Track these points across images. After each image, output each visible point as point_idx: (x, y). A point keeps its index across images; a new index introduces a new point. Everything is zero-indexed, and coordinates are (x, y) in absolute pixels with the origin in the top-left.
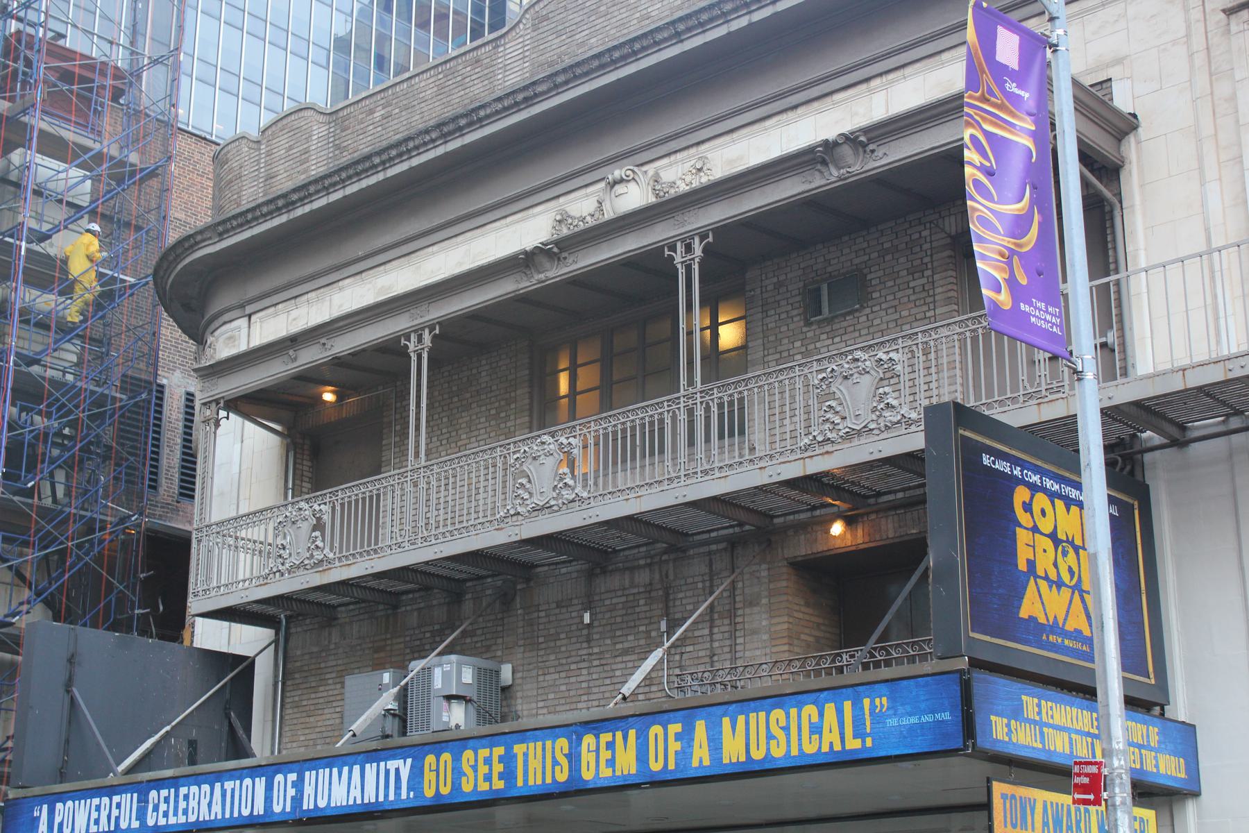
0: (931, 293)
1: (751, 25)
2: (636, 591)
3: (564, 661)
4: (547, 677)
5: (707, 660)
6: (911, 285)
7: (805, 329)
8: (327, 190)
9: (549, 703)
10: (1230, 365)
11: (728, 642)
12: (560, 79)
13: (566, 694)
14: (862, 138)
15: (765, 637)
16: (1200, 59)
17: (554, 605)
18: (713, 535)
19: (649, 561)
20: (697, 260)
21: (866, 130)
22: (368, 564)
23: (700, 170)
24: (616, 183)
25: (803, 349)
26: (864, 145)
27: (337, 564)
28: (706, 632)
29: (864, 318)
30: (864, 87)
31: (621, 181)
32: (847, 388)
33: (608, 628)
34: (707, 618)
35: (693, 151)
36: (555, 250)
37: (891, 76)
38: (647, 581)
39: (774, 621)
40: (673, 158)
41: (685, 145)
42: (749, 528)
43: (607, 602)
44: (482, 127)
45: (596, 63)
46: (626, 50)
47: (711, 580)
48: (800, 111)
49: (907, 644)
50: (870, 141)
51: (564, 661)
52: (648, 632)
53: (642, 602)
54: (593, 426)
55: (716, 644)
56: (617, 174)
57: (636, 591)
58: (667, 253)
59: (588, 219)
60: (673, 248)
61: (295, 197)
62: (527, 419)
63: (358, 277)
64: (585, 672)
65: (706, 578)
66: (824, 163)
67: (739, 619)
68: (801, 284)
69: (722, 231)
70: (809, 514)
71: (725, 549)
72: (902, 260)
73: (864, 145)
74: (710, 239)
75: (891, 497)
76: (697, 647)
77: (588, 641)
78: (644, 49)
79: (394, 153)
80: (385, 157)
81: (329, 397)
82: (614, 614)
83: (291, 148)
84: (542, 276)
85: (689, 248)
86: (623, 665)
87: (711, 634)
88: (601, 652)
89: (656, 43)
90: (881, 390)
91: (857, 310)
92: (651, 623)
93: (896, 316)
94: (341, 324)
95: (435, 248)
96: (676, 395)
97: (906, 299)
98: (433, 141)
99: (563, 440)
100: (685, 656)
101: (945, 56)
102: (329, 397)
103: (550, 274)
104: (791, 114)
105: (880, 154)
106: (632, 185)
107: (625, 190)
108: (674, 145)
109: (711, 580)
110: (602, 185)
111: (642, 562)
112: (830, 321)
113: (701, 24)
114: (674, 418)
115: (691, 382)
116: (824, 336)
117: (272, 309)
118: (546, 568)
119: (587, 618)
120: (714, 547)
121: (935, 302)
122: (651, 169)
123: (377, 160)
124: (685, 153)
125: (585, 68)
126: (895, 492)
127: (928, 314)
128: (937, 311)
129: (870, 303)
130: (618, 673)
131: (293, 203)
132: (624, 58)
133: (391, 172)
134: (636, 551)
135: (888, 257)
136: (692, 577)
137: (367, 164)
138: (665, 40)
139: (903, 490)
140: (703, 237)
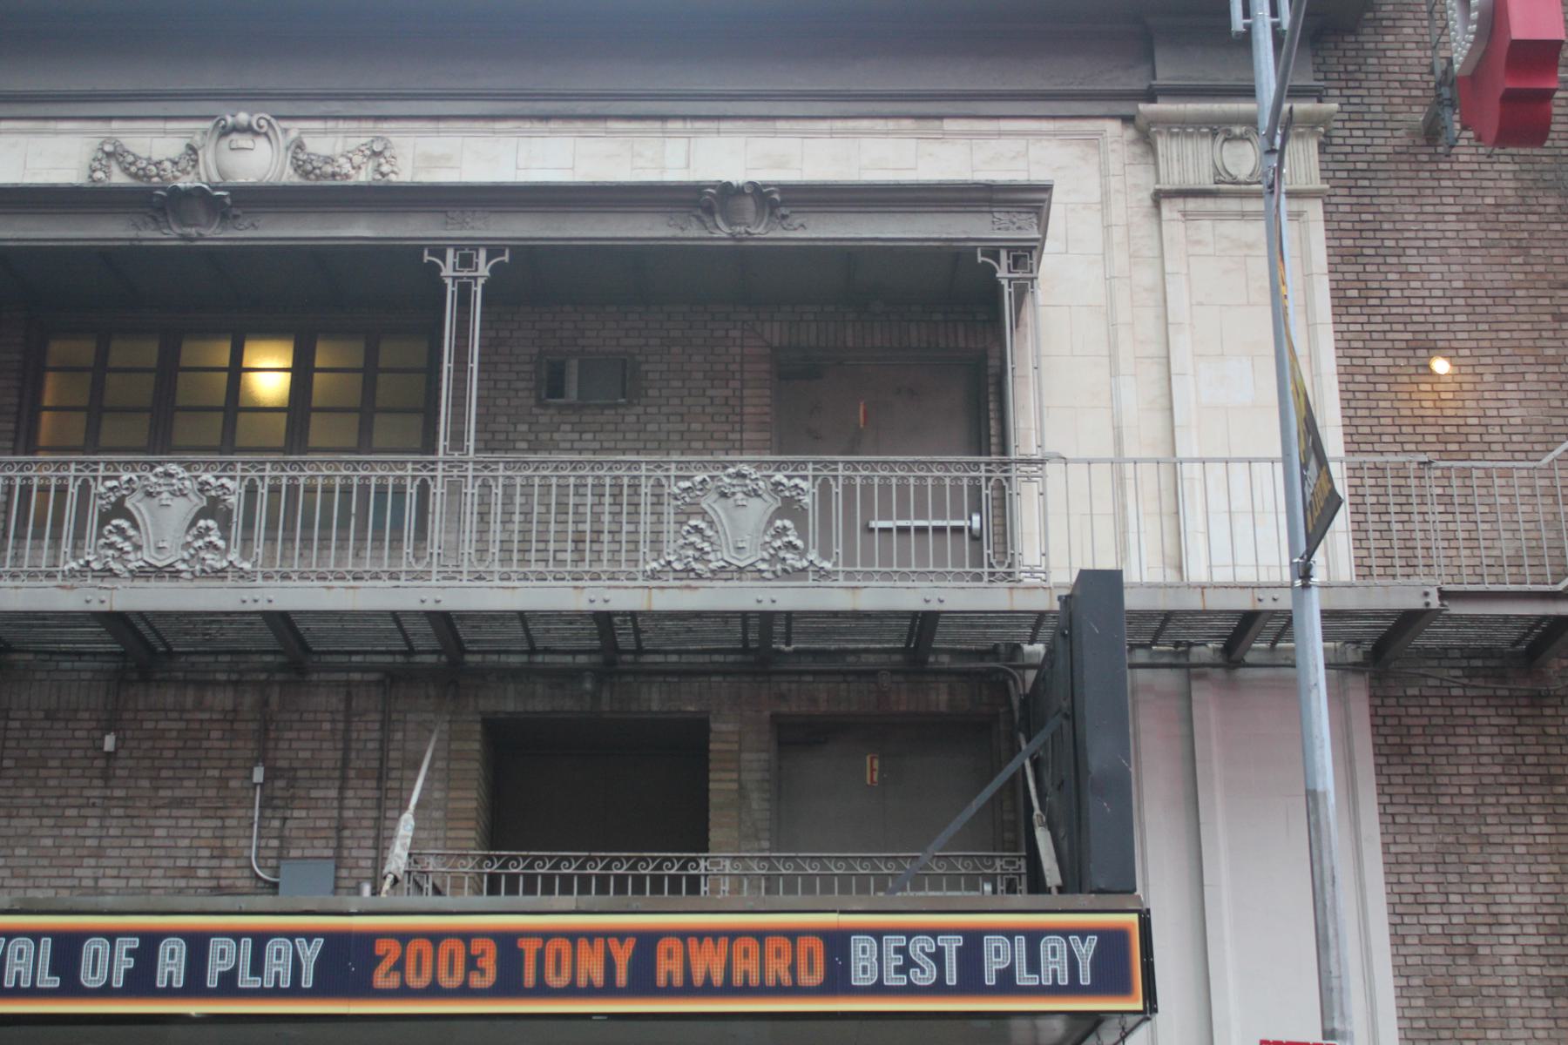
0: (738, 410)
2: (206, 716)
3: (53, 802)
4: (15, 822)
5: (333, 833)
6: (710, 392)
7: (535, 411)
9: (10, 862)
10: (1259, 593)
11: (374, 814)
13: (53, 852)
14: (776, 196)
15: (437, 814)
16: (1118, 234)
17: (41, 715)
18: (355, 658)
19: (234, 677)
20: (481, 281)
21: (785, 188)
23: (376, 154)
24: (237, 129)
25: (532, 437)
26: (774, 206)
28: (333, 793)
29: (633, 418)
30: (657, 125)
31: (248, 130)
32: (726, 510)
33: (147, 763)
34: (337, 774)
35: (369, 125)
36: (228, 201)
37: (699, 125)
38: (229, 705)
39: (453, 794)
40: (331, 124)
41: (356, 112)
42: (440, 659)
43: (149, 725)
47: (348, 721)
48: (553, 125)
49: (778, 858)
50: (783, 203)
51: (53, 802)
52: (223, 782)
53: (214, 734)
54: (268, 471)
55: (348, 814)
56: (243, 117)
57: (206, 716)
58: (427, 258)
59: (167, 165)
62: (11, 426)
64: (94, 823)
65: (340, 717)
66: (709, 210)
67: (391, 784)
68: (535, 350)
69: (527, 255)
70: (524, 658)
71: (379, 683)
72: (696, 358)
73: (774, 206)
74: (506, 258)
75: (659, 658)
76: (312, 813)
77: (106, 777)
82: (159, 744)
84: (193, 231)
85: (466, 261)
86: (172, 822)
87: (341, 798)
88: (126, 798)
90: (779, 523)
91: (622, 405)
92: (229, 768)
93: (683, 427)
96: (431, 458)
97: (699, 409)
99: (207, 477)
100: (289, 823)
101: (780, 125)
103: (208, 233)
104: (538, 126)
105: (797, 222)
106: (262, 143)
107: (249, 144)
109: (348, 721)
110: (209, 125)
111: (221, 677)
114: (424, 490)
115: (457, 440)
116: (568, 427)
118: (30, 657)
119: (109, 743)
120: (356, 676)
121: (742, 422)
122: (295, 128)
124: (354, 125)
126: (666, 653)
127: (731, 436)
128: (746, 436)
129: (644, 401)
130: (160, 832)
134: (211, 659)
135: (674, 350)
136: (315, 712)
139: (679, 652)
140: (493, 252)
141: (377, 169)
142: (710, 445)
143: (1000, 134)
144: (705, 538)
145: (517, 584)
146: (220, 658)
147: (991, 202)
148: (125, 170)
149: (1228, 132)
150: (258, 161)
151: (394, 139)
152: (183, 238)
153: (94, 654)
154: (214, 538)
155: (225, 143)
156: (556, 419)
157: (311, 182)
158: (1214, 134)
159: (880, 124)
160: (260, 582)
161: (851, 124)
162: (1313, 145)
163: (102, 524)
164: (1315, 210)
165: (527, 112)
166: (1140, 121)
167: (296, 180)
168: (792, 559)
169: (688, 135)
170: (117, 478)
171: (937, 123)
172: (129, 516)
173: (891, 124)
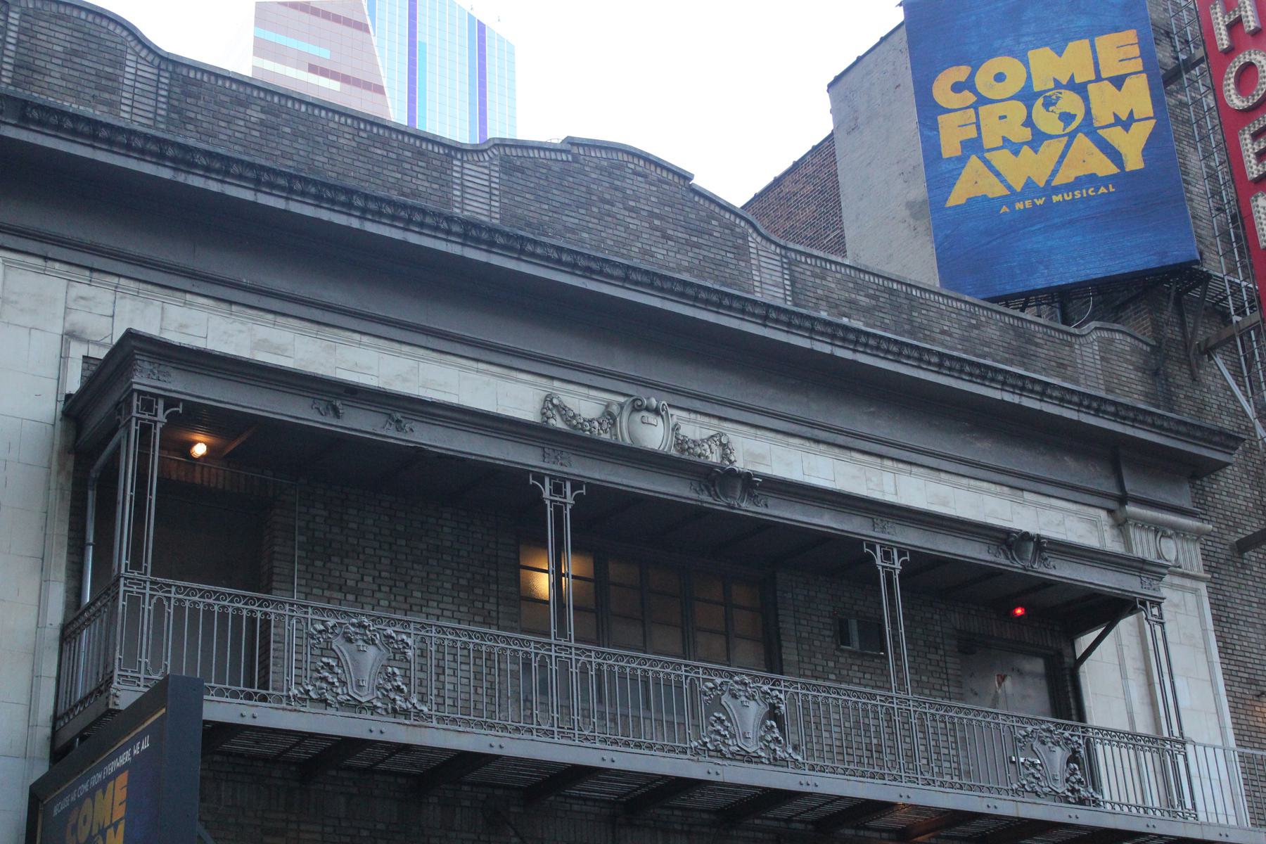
1: (832, 356)
8: (258, 185)
12: (634, 276)
19: (686, 828)
21: (1052, 542)
22: (496, 742)
27: (435, 723)
30: (879, 460)
31: (656, 412)
35: (715, 422)
40: (693, 416)
44: (518, 259)
45: (679, 288)
46: (715, 298)
48: (822, 447)
56: (654, 402)
59: (596, 424)
60: (873, 548)
61: (203, 161)
63: (224, 306)
66: (1010, 547)
78: (730, 308)
79: (389, 210)
80: (372, 206)
81: (200, 450)
83: (75, 53)
89: (743, 311)
94: (441, 412)
95: (365, 339)
98: (449, 232)
101: (943, 475)
102: (200, 450)
103: (744, 505)
104: (814, 446)
106: (660, 419)
108: (697, 405)
110: (622, 399)
112: (861, 655)
113: (789, 324)
117: (40, 262)
120: (760, 835)
123: (359, 202)
124: (706, 419)
125: (667, 285)
131: (195, 166)
132: (707, 302)
133: (371, 227)
137: (343, 198)
138: (753, 315)
141: (725, 456)
142: (934, 693)
143: (1051, 507)
144: (726, 728)
145: (807, 772)
146: (676, 813)
147: (1141, 570)
148: (567, 421)
149: (1164, 532)
150: (654, 435)
151: (731, 437)
152: (729, 506)
153: (595, 800)
154: (777, 734)
155: (637, 417)
156: (849, 661)
157: (686, 456)
158: (1156, 532)
159: (992, 487)
160: (807, 772)
161: (979, 484)
162: (1198, 546)
163: (707, 717)
164: (1202, 587)
165: (809, 435)
166: (1118, 514)
167: (674, 452)
168: (1083, 793)
169: (895, 472)
170: (712, 681)
171: (1020, 493)
172: (725, 712)
173: (998, 488)
